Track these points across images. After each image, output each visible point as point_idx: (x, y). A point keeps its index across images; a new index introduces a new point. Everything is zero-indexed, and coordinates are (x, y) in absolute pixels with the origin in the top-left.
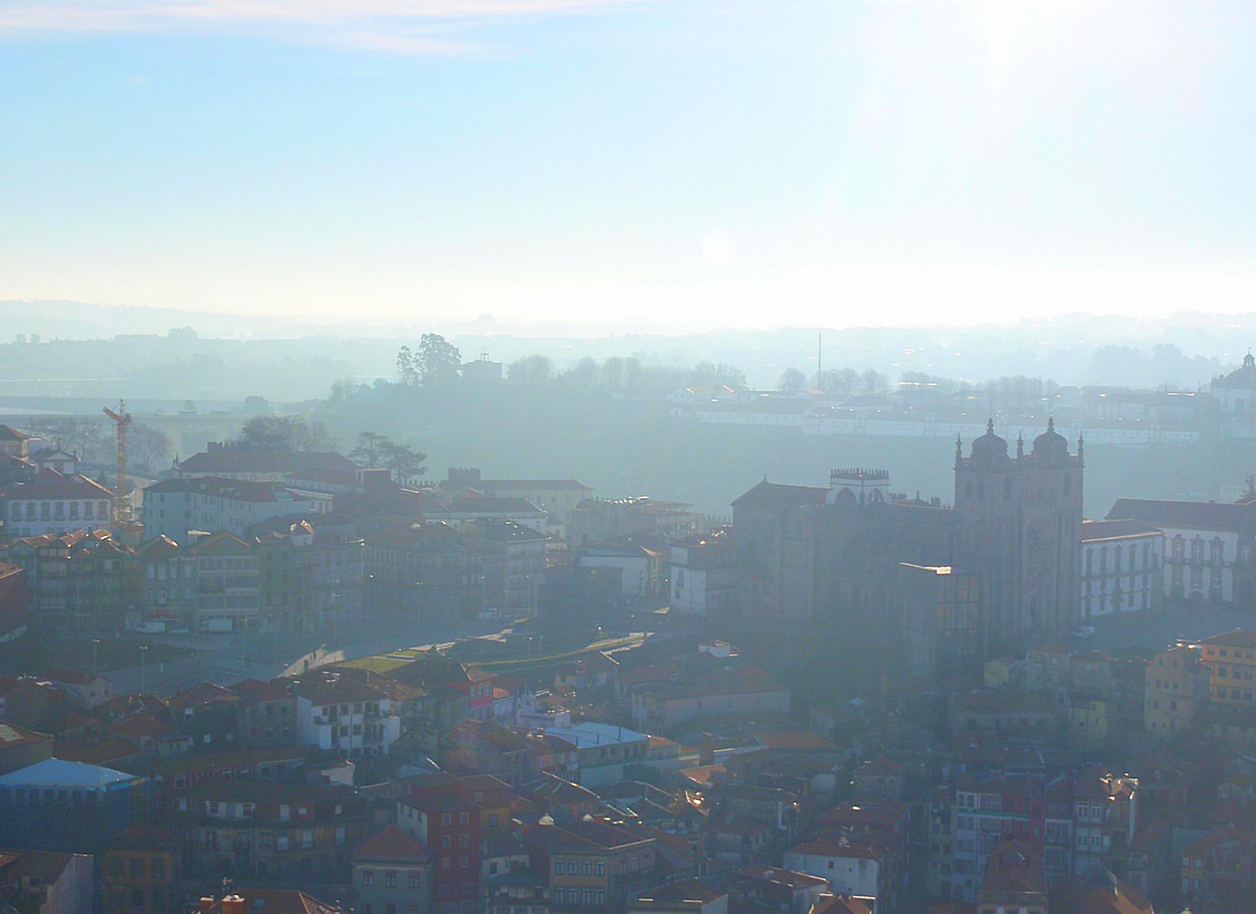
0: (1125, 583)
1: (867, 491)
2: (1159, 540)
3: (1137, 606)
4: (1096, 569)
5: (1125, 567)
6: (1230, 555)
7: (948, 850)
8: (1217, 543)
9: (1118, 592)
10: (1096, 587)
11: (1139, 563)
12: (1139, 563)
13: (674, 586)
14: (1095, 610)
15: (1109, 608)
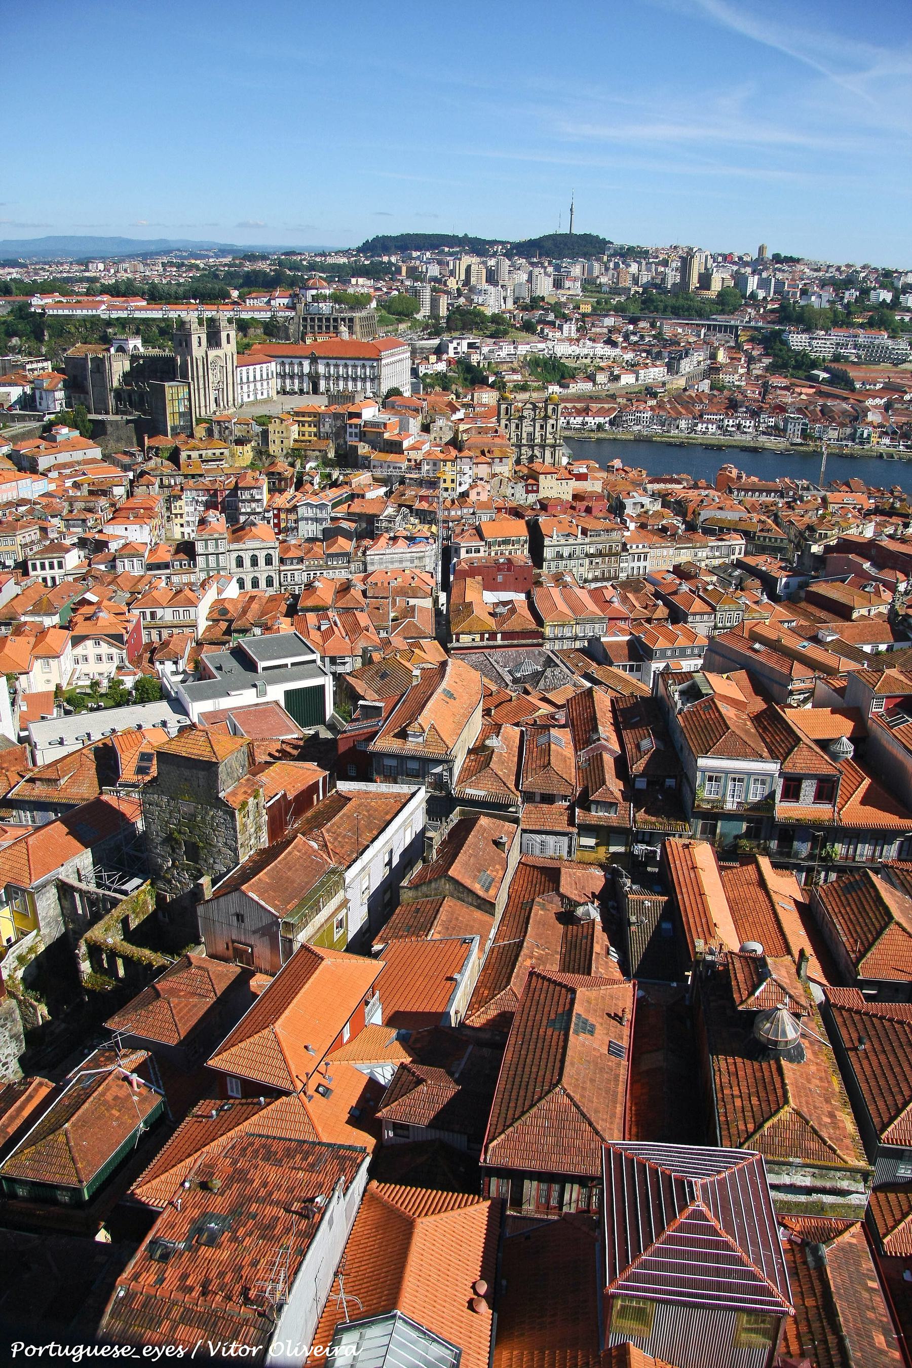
0: (258, 384)
1: (131, 347)
2: (273, 364)
3: (265, 396)
4: (245, 380)
5: (258, 378)
6: (306, 370)
7: (181, 515)
8: (301, 364)
9: (256, 389)
10: (245, 387)
11: (265, 377)
12: (265, 377)
13: (38, 400)
14: (246, 399)
15: (252, 398)
